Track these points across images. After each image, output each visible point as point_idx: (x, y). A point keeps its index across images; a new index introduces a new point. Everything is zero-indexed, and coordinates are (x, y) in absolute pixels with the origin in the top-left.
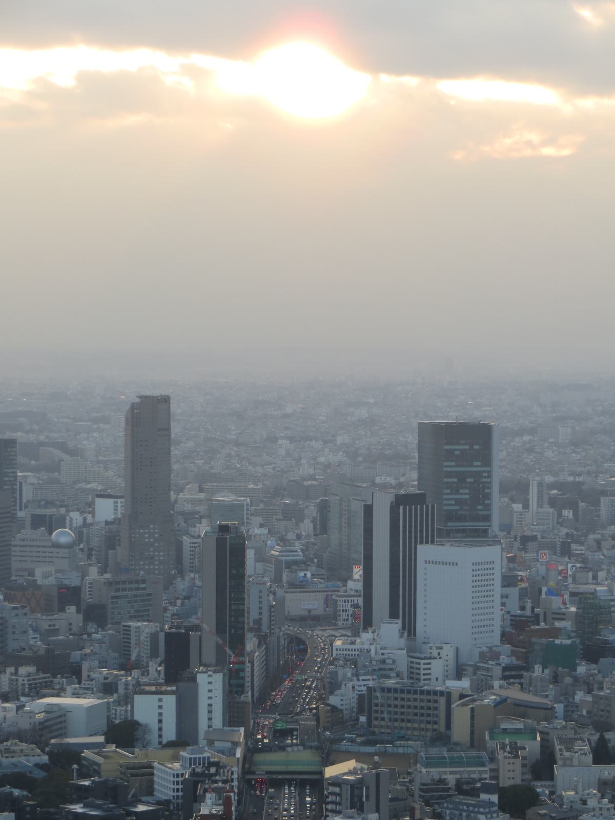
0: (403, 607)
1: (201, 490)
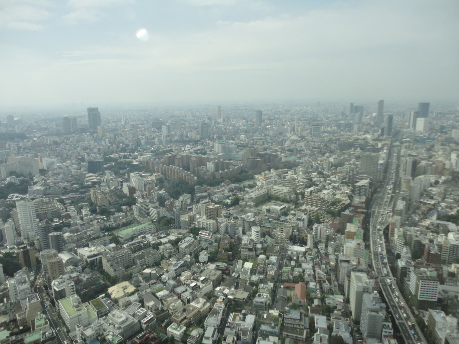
0: (414, 125)
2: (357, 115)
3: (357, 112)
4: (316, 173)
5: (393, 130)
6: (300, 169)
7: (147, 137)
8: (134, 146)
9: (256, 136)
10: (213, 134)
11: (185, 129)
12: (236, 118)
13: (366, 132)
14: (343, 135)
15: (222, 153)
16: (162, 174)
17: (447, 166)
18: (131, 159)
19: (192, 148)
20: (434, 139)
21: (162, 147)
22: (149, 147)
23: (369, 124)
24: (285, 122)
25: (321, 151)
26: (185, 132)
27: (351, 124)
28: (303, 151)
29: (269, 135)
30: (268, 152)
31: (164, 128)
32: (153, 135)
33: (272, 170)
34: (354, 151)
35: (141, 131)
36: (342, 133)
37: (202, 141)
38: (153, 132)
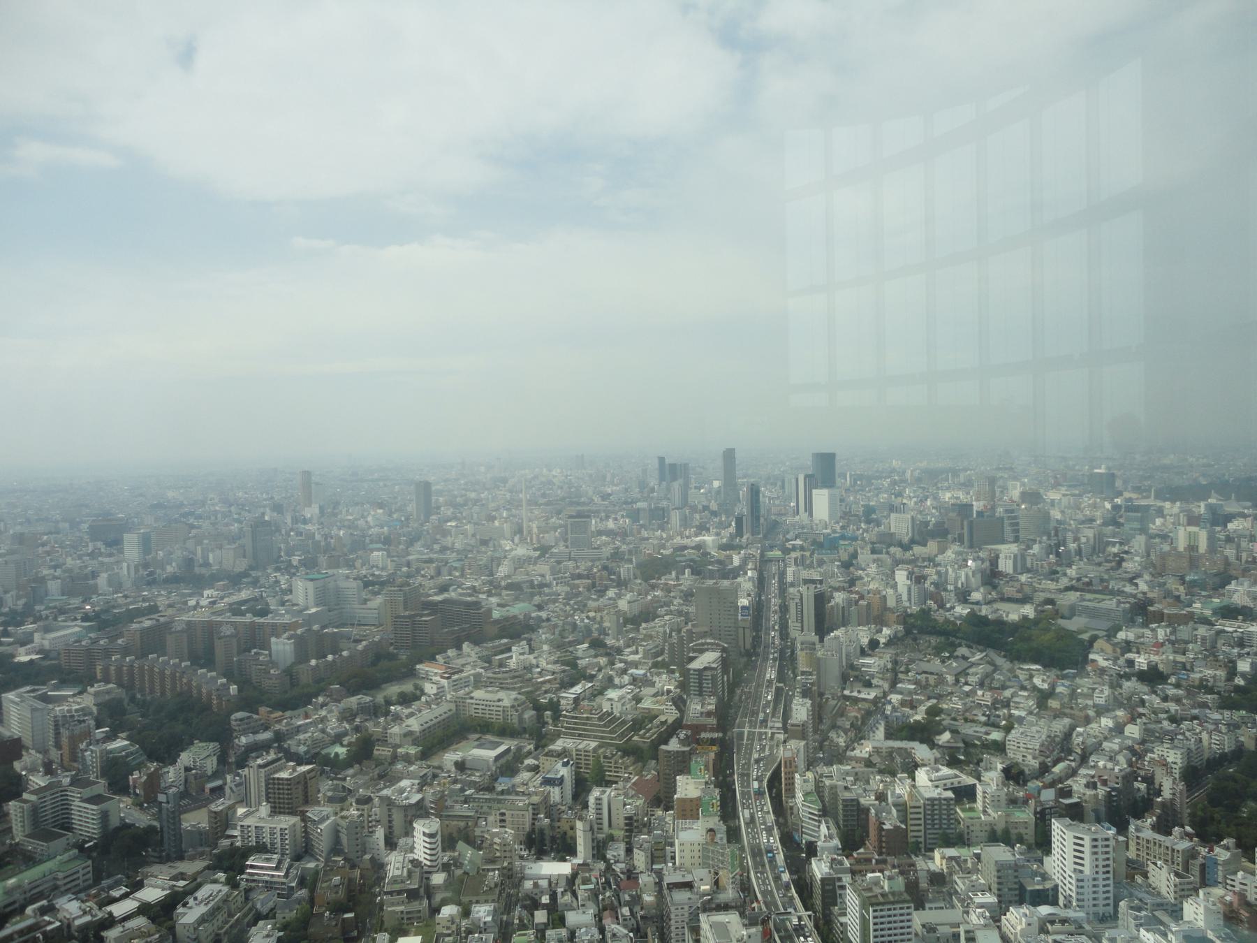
2: (676, 485)
3: (674, 479)
4: (586, 645)
5: (762, 520)
6: (543, 635)
7: (70, 571)
8: (22, 602)
9: (417, 553)
10: (290, 553)
11: (199, 543)
12: (357, 504)
13: (702, 528)
14: (647, 539)
15: (317, 605)
16: (120, 685)
17: (891, 603)
18: (9, 644)
19: (222, 598)
20: (855, 539)
21: (120, 601)
22: (75, 602)
23: (706, 508)
24: (496, 510)
25: (594, 585)
26: (199, 548)
28: (548, 585)
29: (452, 549)
30: (452, 595)
31: (131, 544)
32: (92, 565)
33: (466, 646)
34: (678, 579)
35: (48, 553)
36: (645, 534)
37: (254, 573)
38: (92, 555)
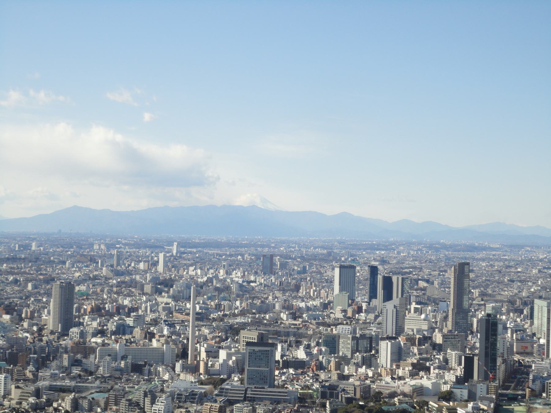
1: (482, 300)
5: (499, 361)
13: (419, 368)
14: (347, 378)
23: (425, 339)
27: (371, 339)
